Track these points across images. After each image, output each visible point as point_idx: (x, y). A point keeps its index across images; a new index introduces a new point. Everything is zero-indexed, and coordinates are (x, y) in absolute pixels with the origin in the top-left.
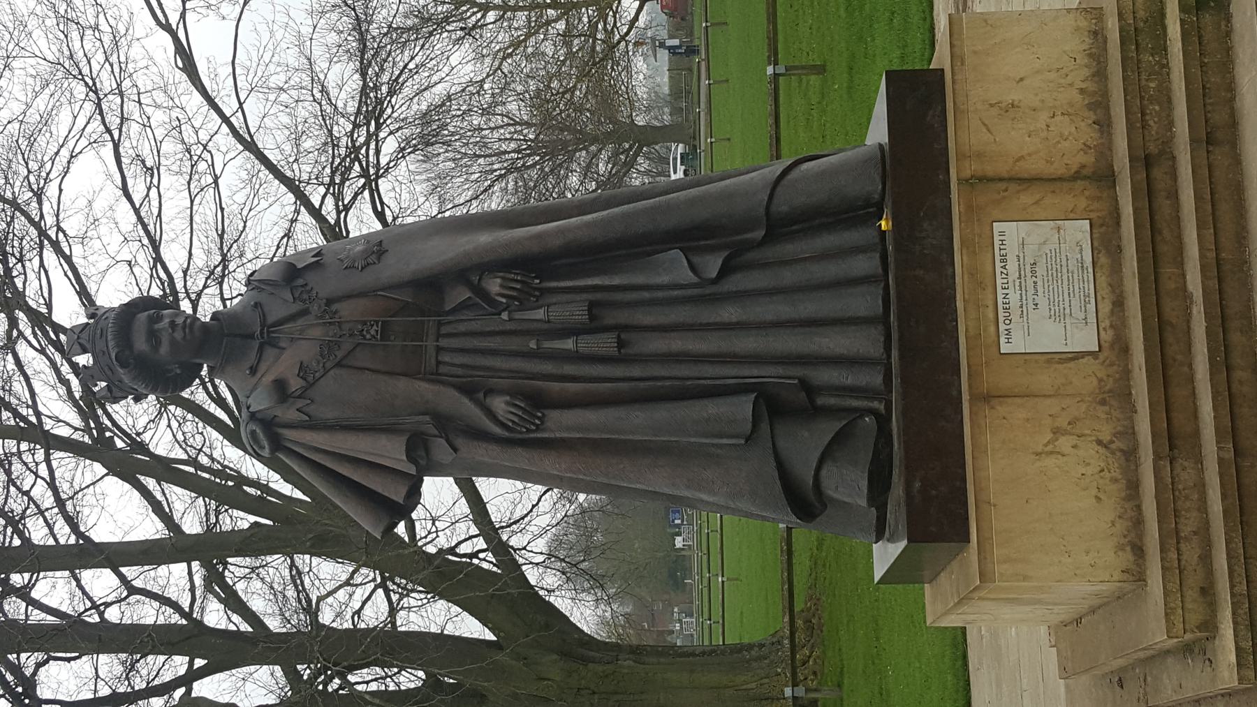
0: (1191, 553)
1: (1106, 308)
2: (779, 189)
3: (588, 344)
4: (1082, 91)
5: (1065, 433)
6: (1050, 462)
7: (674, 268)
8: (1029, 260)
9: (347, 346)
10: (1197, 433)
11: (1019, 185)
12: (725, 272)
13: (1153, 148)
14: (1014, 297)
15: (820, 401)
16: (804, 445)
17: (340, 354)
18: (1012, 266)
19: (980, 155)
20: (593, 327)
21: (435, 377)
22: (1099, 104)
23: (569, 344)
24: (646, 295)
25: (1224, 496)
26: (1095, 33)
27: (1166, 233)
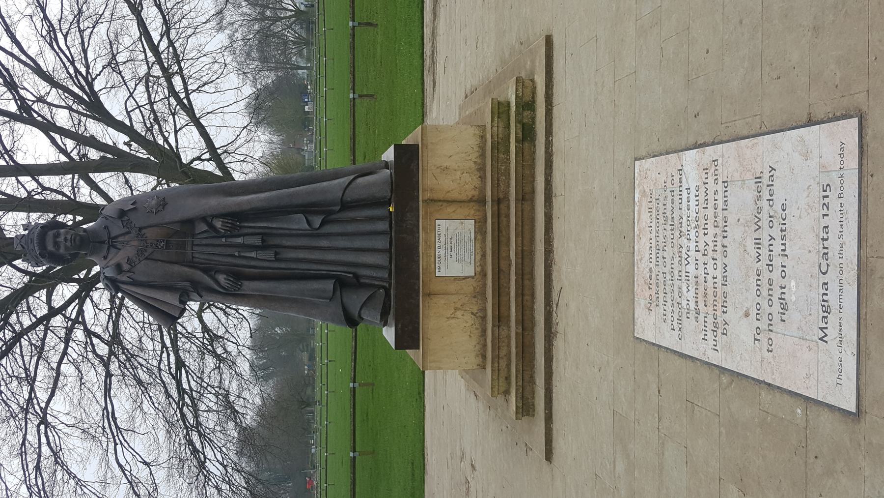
0: (503, 363)
1: (478, 257)
2: (347, 191)
3: (262, 255)
5: (459, 309)
6: (452, 321)
7: (299, 222)
8: (450, 237)
9: (150, 250)
10: (509, 316)
11: (446, 204)
12: (322, 224)
13: (501, 196)
14: (442, 252)
15: (362, 281)
16: (355, 300)
17: (147, 254)
18: (442, 239)
19: (432, 190)
20: (264, 247)
21: (192, 265)
22: (482, 169)
23: (253, 255)
24: (287, 232)
25: (516, 347)
26: (482, 137)
27: (504, 233)
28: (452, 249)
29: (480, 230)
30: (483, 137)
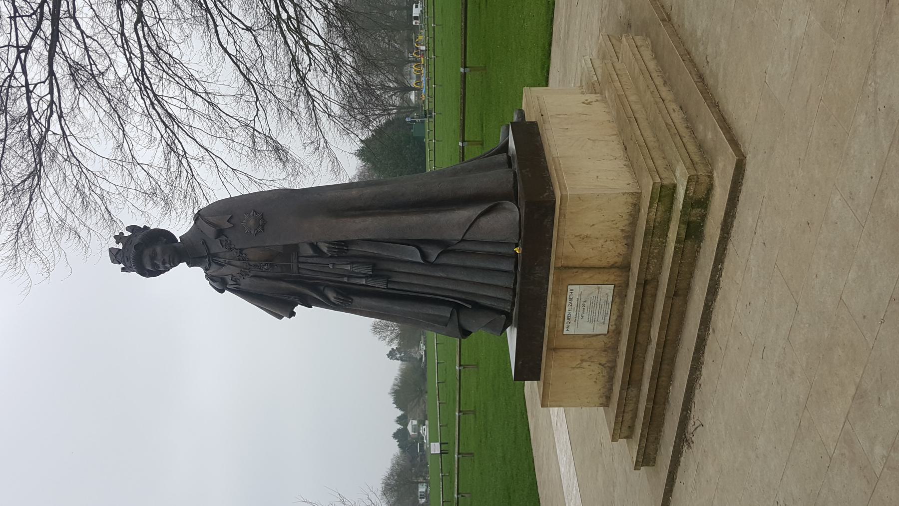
0: (628, 417)
1: (614, 318)
4: (623, 231)
5: (586, 361)
6: (577, 370)
8: (583, 300)
13: (649, 277)
14: (573, 314)
18: (574, 302)
19: (567, 257)
22: (629, 238)
26: (635, 205)
27: (647, 310)
28: (584, 311)
29: (620, 294)
30: (636, 207)
